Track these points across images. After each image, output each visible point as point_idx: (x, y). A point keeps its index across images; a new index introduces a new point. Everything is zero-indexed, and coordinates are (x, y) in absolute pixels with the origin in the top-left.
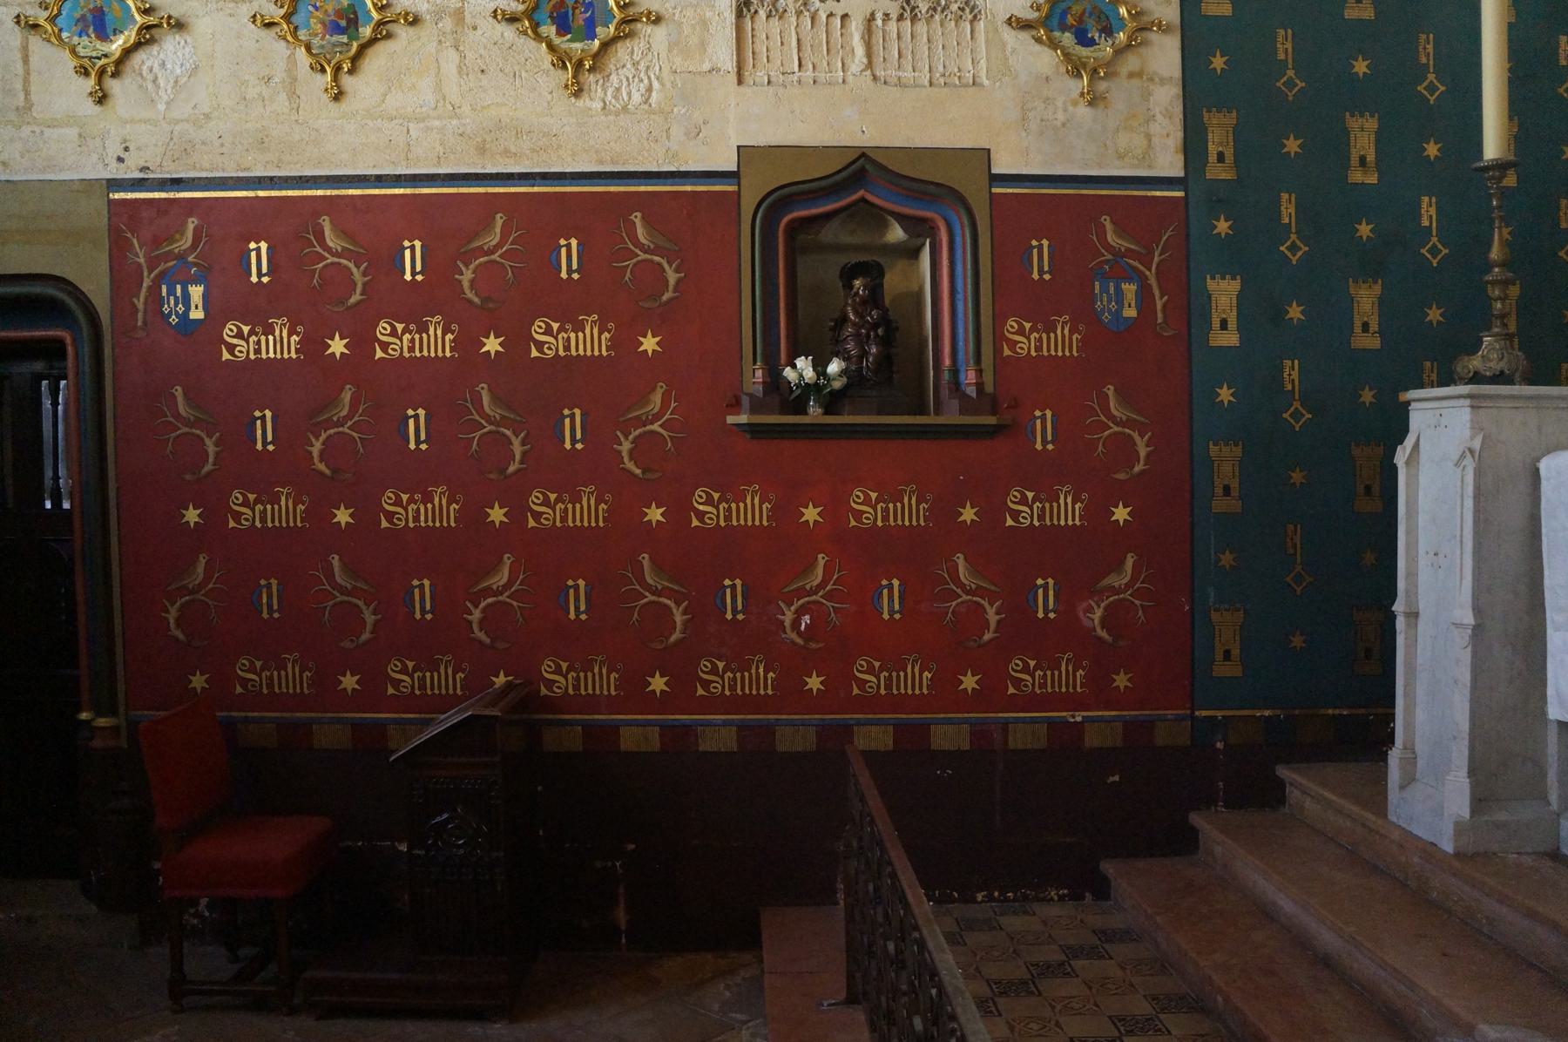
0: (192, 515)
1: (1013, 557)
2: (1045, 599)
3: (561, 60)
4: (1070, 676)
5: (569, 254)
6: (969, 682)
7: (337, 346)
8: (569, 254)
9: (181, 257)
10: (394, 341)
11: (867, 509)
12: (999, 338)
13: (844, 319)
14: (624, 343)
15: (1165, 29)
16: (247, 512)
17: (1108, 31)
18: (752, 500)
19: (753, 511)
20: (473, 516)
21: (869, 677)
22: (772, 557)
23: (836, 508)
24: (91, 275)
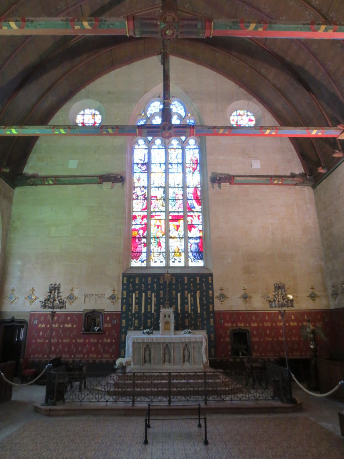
1: (104, 345)
2: (107, 348)
3: (70, 302)
4: (108, 356)
5: (69, 318)
6: (99, 356)
8: (69, 318)
9: (36, 318)
11: (92, 340)
12: (104, 325)
13: (91, 324)
14: (73, 326)
15: (120, 298)
16: (39, 341)
17: (115, 298)
18: (82, 340)
20: (58, 341)
21: (91, 356)
22: (83, 345)
23: (89, 341)
24: (28, 320)
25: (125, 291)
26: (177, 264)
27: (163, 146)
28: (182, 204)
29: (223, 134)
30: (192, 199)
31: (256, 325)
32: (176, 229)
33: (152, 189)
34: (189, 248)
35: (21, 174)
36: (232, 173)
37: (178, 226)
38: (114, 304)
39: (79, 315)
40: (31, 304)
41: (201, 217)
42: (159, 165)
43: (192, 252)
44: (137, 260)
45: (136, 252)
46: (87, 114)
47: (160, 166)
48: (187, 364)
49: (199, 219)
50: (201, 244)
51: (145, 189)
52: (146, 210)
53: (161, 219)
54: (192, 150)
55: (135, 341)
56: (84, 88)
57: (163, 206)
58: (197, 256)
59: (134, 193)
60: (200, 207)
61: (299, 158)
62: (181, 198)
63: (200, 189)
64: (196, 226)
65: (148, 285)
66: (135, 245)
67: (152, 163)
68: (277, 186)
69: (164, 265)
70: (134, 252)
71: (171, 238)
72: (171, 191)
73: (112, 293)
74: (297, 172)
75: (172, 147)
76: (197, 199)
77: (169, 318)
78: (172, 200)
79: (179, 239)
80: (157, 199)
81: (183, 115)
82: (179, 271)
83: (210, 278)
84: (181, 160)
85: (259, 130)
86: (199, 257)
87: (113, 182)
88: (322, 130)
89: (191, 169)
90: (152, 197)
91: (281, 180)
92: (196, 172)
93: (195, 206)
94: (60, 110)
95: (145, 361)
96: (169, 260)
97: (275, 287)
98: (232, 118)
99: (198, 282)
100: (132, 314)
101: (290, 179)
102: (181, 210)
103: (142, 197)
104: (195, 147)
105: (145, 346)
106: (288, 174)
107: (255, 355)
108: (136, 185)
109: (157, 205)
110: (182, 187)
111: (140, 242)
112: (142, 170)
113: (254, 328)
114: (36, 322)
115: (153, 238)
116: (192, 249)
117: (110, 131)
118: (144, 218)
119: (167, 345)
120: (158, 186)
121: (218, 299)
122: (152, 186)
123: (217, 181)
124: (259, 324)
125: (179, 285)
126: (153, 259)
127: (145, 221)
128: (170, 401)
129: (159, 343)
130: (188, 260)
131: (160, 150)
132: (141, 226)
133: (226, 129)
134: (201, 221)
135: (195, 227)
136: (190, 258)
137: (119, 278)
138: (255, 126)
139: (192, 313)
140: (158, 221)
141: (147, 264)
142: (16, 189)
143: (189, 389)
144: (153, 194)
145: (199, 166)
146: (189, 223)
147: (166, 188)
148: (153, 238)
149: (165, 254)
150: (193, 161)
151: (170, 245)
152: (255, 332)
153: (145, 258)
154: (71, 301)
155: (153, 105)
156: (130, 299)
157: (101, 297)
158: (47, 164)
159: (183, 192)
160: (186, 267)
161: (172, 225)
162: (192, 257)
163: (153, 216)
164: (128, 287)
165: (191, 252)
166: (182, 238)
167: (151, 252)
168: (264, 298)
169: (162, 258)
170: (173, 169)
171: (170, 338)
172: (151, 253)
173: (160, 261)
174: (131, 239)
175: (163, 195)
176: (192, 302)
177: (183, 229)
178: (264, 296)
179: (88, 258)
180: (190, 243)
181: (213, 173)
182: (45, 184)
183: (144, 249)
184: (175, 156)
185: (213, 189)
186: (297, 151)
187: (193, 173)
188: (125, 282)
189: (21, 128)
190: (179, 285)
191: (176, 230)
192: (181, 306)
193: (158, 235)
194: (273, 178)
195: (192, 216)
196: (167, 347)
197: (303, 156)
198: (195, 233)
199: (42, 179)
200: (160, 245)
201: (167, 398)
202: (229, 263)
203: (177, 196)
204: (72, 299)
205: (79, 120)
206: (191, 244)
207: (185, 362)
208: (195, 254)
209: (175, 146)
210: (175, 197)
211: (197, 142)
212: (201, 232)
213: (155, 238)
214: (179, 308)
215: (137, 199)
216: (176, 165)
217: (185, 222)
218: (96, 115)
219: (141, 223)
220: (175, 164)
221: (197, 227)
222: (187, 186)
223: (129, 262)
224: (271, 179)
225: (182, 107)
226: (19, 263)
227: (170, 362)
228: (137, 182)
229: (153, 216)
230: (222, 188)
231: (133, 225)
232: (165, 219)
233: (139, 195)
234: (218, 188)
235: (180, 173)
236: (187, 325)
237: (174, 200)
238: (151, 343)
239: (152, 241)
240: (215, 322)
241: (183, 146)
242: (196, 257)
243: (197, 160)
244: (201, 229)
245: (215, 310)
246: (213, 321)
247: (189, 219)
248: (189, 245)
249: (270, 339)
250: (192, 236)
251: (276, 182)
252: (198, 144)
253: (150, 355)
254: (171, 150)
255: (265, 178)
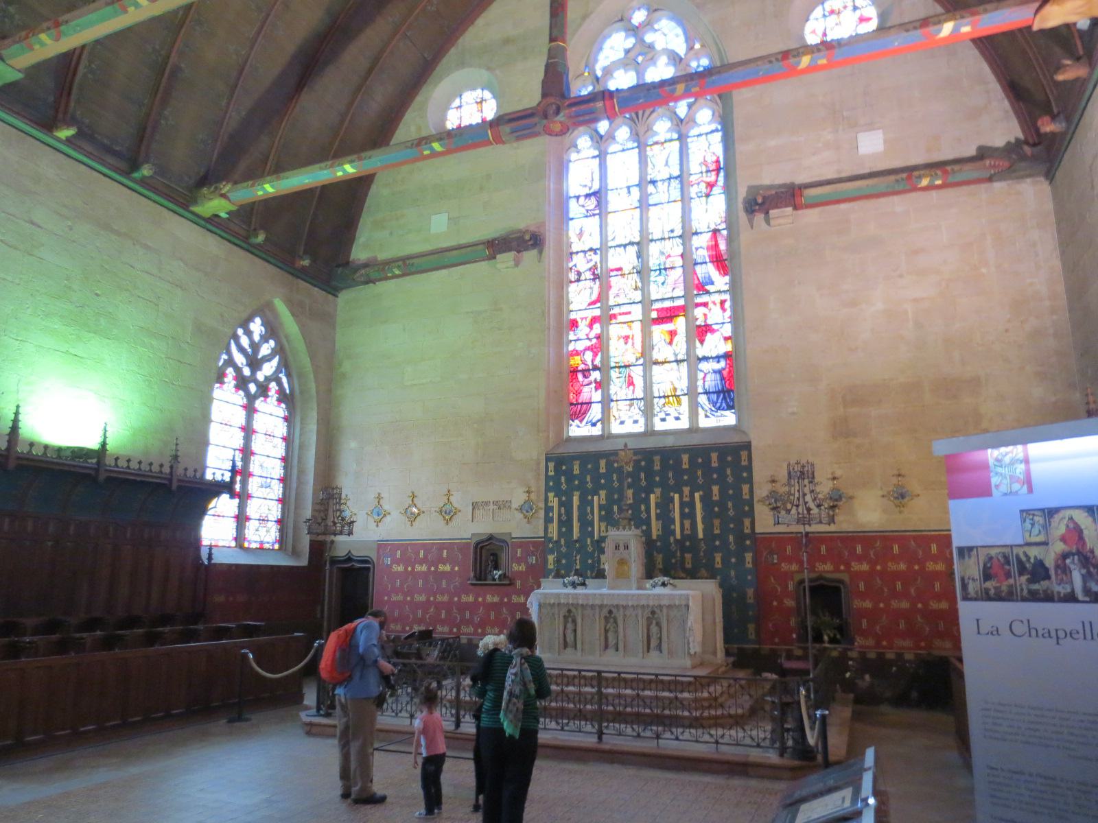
0: (386, 598)
3: (445, 519)
7: (410, 569)
10: (418, 568)
11: (489, 599)
14: (453, 569)
15: (541, 509)
16: (395, 598)
17: (532, 510)
19: (471, 599)
20: (428, 600)
22: (473, 607)
25: (551, 491)
26: (671, 425)
27: (634, 141)
28: (682, 278)
29: (812, 69)
30: (705, 263)
31: (865, 567)
32: (668, 341)
33: (611, 251)
34: (700, 383)
35: (347, 263)
36: (801, 179)
37: (673, 334)
38: (529, 522)
39: (463, 547)
40: (377, 526)
41: (727, 305)
42: (626, 190)
43: (707, 393)
44: (581, 421)
45: (578, 404)
46: (467, 103)
47: (629, 192)
48: (654, 653)
49: (724, 310)
50: (730, 372)
51: (596, 253)
52: (598, 305)
53: (632, 322)
54: (704, 136)
55: (542, 601)
56: (453, 45)
57: (636, 289)
58: (720, 401)
59: (571, 269)
60: (727, 279)
61: (1008, 97)
62: (679, 262)
63: (725, 233)
64: (715, 327)
65: (600, 476)
66: (576, 389)
67: (609, 188)
68: (934, 193)
69: (642, 430)
70: (575, 405)
71: (657, 363)
72: (654, 249)
73: (525, 497)
74: (999, 141)
75: (655, 139)
76: (717, 261)
77: (626, 551)
78: (658, 272)
79: (675, 364)
80: (623, 275)
81: (681, 49)
82: (670, 442)
83: (744, 454)
84: (678, 167)
85: (781, 63)
86: (724, 405)
87: (519, 252)
88: (973, 14)
89: (703, 186)
90: (612, 270)
91: (939, 172)
92: (716, 190)
93: (714, 279)
94: (409, 111)
95: (566, 645)
96: (653, 415)
97: (789, 473)
98: (809, 27)
99: (685, 466)
100: (676, 540)
101: (968, 167)
102: (680, 292)
103: (589, 275)
104: (713, 127)
105: (563, 612)
106: (971, 151)
107: (859, 641)
108: (574, 249)
109: (623, 289)
110: (680, 237)
111: (586, 381)
112: (587, 211)
113: (858, 575)
114: (389, 561)
115: (615, 367)
116: (707, 387)
117: (436, 146)
118: (595, 322)
119: (610, 612)
120: (624, 243)
121: (764, 504)
122: (610, 244)
123: (757, 207)
124: (873, 564)
125: (670, 475)
126: (617, 417)
127: (597, 328)
128: (600, 734)
129: (593, 607)
130: (697, 414)
131: (627, 152)
132: (588, 343)
133: (692, 79)
134: (728, 313)
135: (713, 331)
136: (703, 408)
137: (538, 464)
138: (881, 29)
139: (563, 541)
140: (625, 325)
141: (603, 429)
142: (340, 295)
143: (641, 710)
144: (613, 263)
145: (722, 174)
146: (698, 323)
147: (641, 246)
148: (615, 367)
149: (643, 403)
150: (707, 166)
151: (654, 381)
152: (862, 586)
153: (599, 416)
154: (448, 517)
155: (607, 45)
156: (589, 509)
157: (504, 506)
158: (391, 234)
159: (684, 249)
160: (694, 430)
161: (659, 332)
162: (707, 406)
163: (614, 316)
164: (558, 484)
165: (704, 393)
166: (683, 361)
167: (612, 401)
168: (889, 499)
169: (636, 413)
170: (657, 194)
171: (613, 595)
172: (612, 404)
173: (632, 420)
174: (566, 375)
175: (635, 262)
176: (689, 515)
177: (685, 339)
178: (889, 493)
179: (475, 426)
180: (701, 371)
181: (748, 187)
182: (387, 278)
183: (597, 396)
184: (664, 160)
185: (752, 227)
186: (999, 80)
187: (708, 195)
188: (551, 473)
189: (278, 179)
190: (670, 475)
191: (669, 344)
192: (703, 523)
193: (626, 361)
194: (916, 173)
195: (705, 305)
196: (610, 615)
197: (1016, 91)
198: (715, 345)
199: (381, 267)
200: (631, 383)
201: (593, 726)
202: (793, 413)
203: (670, 259)
204: (449, 514)
205: (452, 121)
206: (705, 375)
207: (651, 651)
208: (714, 397)
209: (661, 138)
210: (665, 264)
211: (717, 114)
212: (729, 341)
213: (620, 367)
214: (700, 527)
215: (578, 280)
216: (666, 184)
217: (690, 321)
218: (485, 100)
219: (587, 335)
220: (663, 180)
221: (718, 330)
222: (694, 231)
223: (561, 428)
224: (909, 178)
225: (679, 31)
226: (353, 445)
227: (617, 650)
228: (577, 239)
229: (614, 316)
230: (772, 222)
231: (571, 341)
232: (641, 321)
233: (581, 271)
234: (763, 224)
235: (675, 201)
236: (720, 566)
237: (663, 270)
238: (576, 606)
239: (614, 374)
240: (755, 561)
241: (682, 128)
242: (718, 405)
243: (717, 161)
244: (728, 334)
245: (758, 530)
246: (753, 557)
247: (699, 312)
248: (700, 375)
249: (905, 605)
250: (706, 355)
251: (925, 182)
252: (719, 119)
253: (575, 631)
254: (653, 147)
255: (893, 178)
